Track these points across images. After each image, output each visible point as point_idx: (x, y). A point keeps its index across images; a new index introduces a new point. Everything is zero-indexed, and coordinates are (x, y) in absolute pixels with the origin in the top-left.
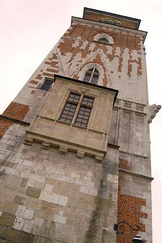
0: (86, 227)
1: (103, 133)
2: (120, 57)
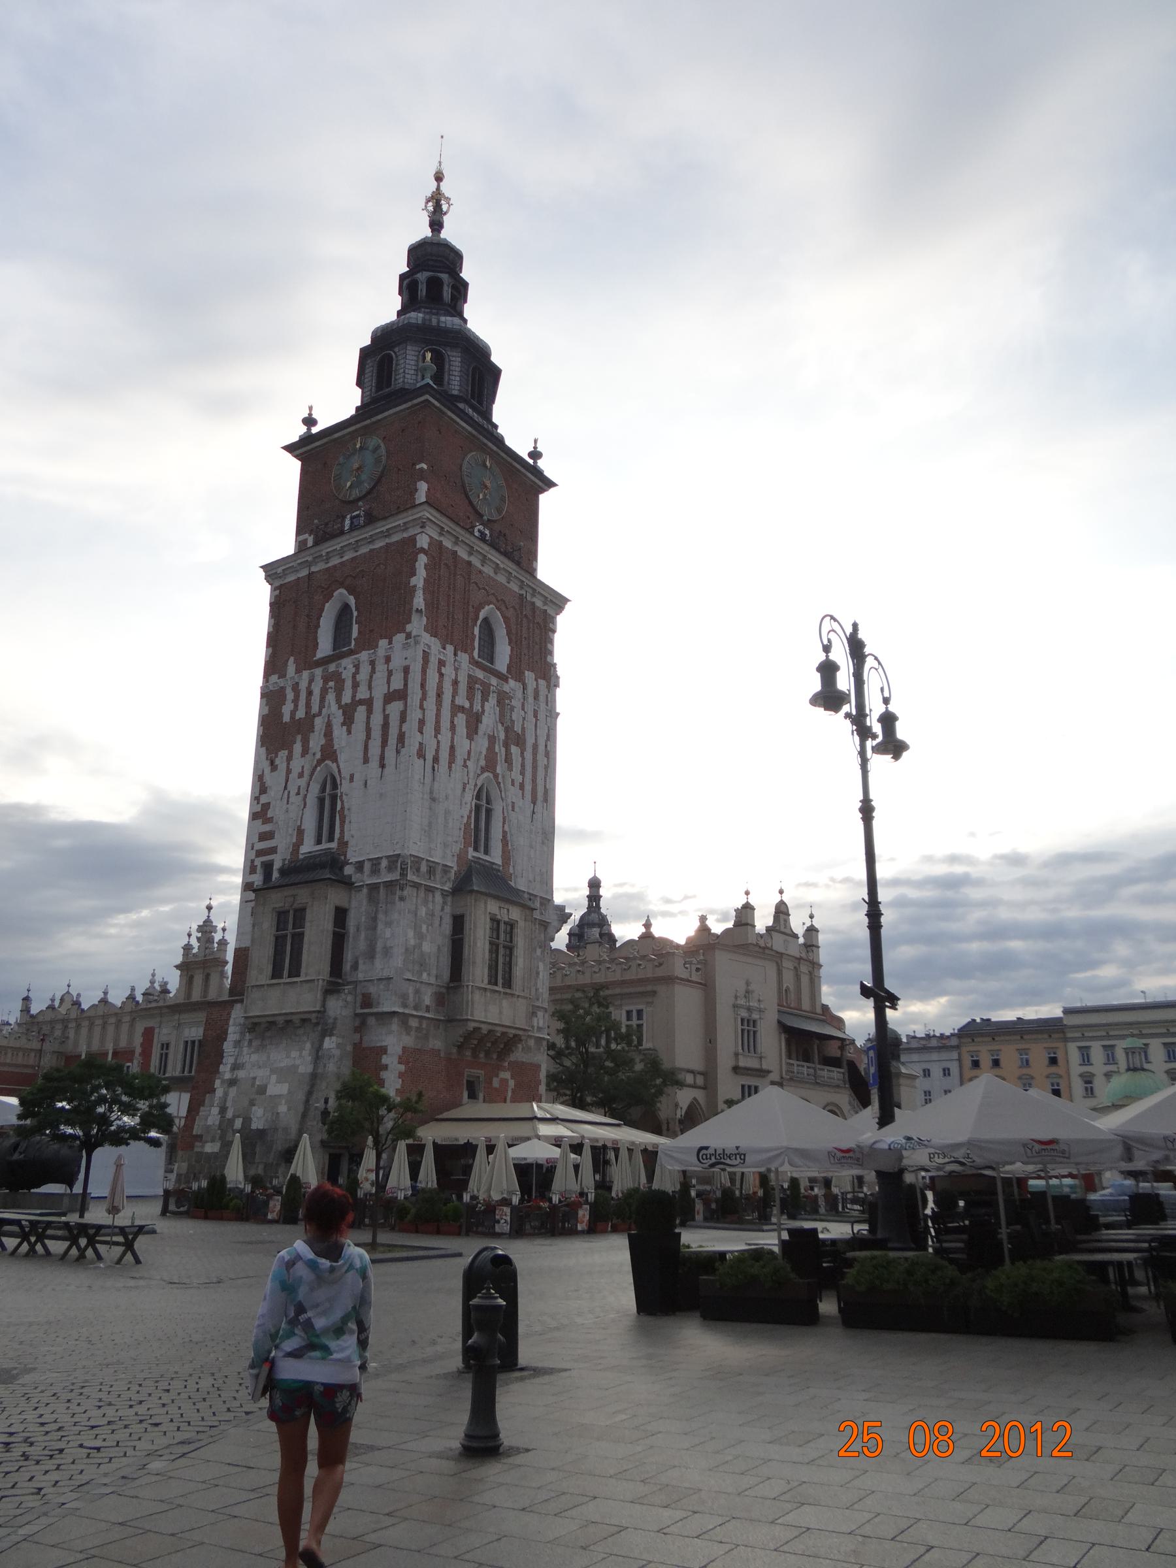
0: (301, 1108)
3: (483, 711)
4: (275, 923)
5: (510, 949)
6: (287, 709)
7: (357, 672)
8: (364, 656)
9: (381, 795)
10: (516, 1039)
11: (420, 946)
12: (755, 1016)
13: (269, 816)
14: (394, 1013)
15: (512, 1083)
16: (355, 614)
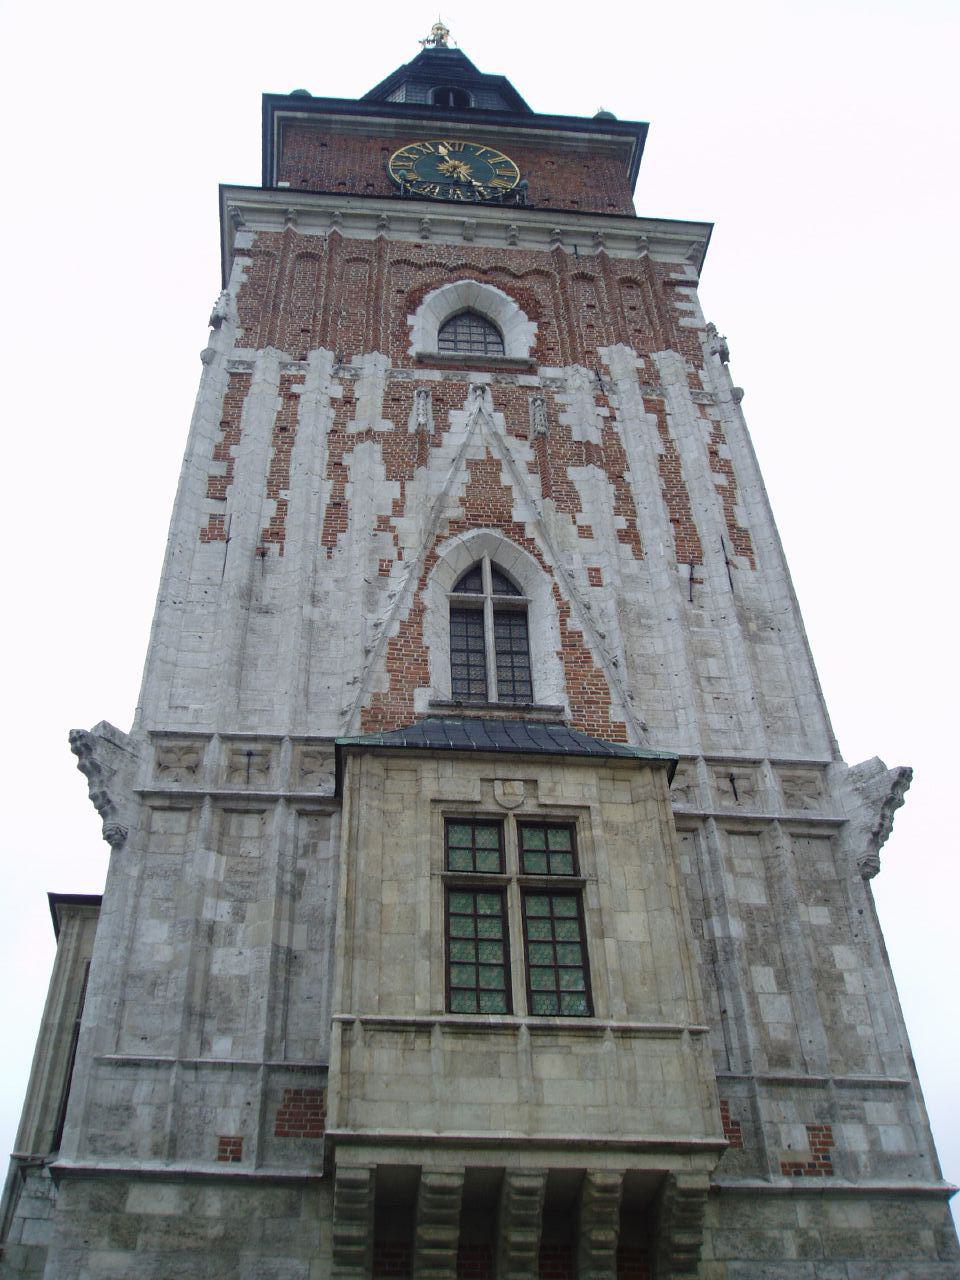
3: (443, 426)
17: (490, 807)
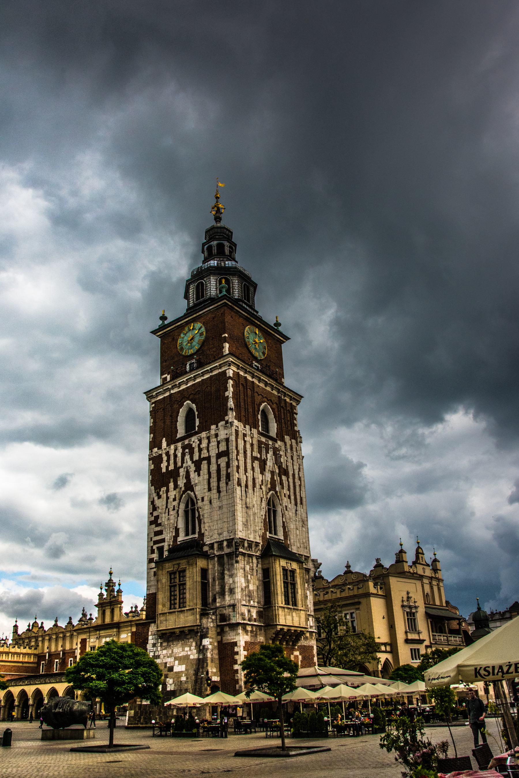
1: (193, 609)
2: (206, 455)
3: (267, 459)
4: (169, 579)
5: (294, 585)
6: (164, 465)
7: (200, 443)
8: (204, 435)
9: (220, 507)
10: (302, 633)
11: (248, 586)
12: (414, 611)
13: (159, 521)
14: (239, 624)
15: (300, 657)
16: (196, 413)
17: (286, 568)
